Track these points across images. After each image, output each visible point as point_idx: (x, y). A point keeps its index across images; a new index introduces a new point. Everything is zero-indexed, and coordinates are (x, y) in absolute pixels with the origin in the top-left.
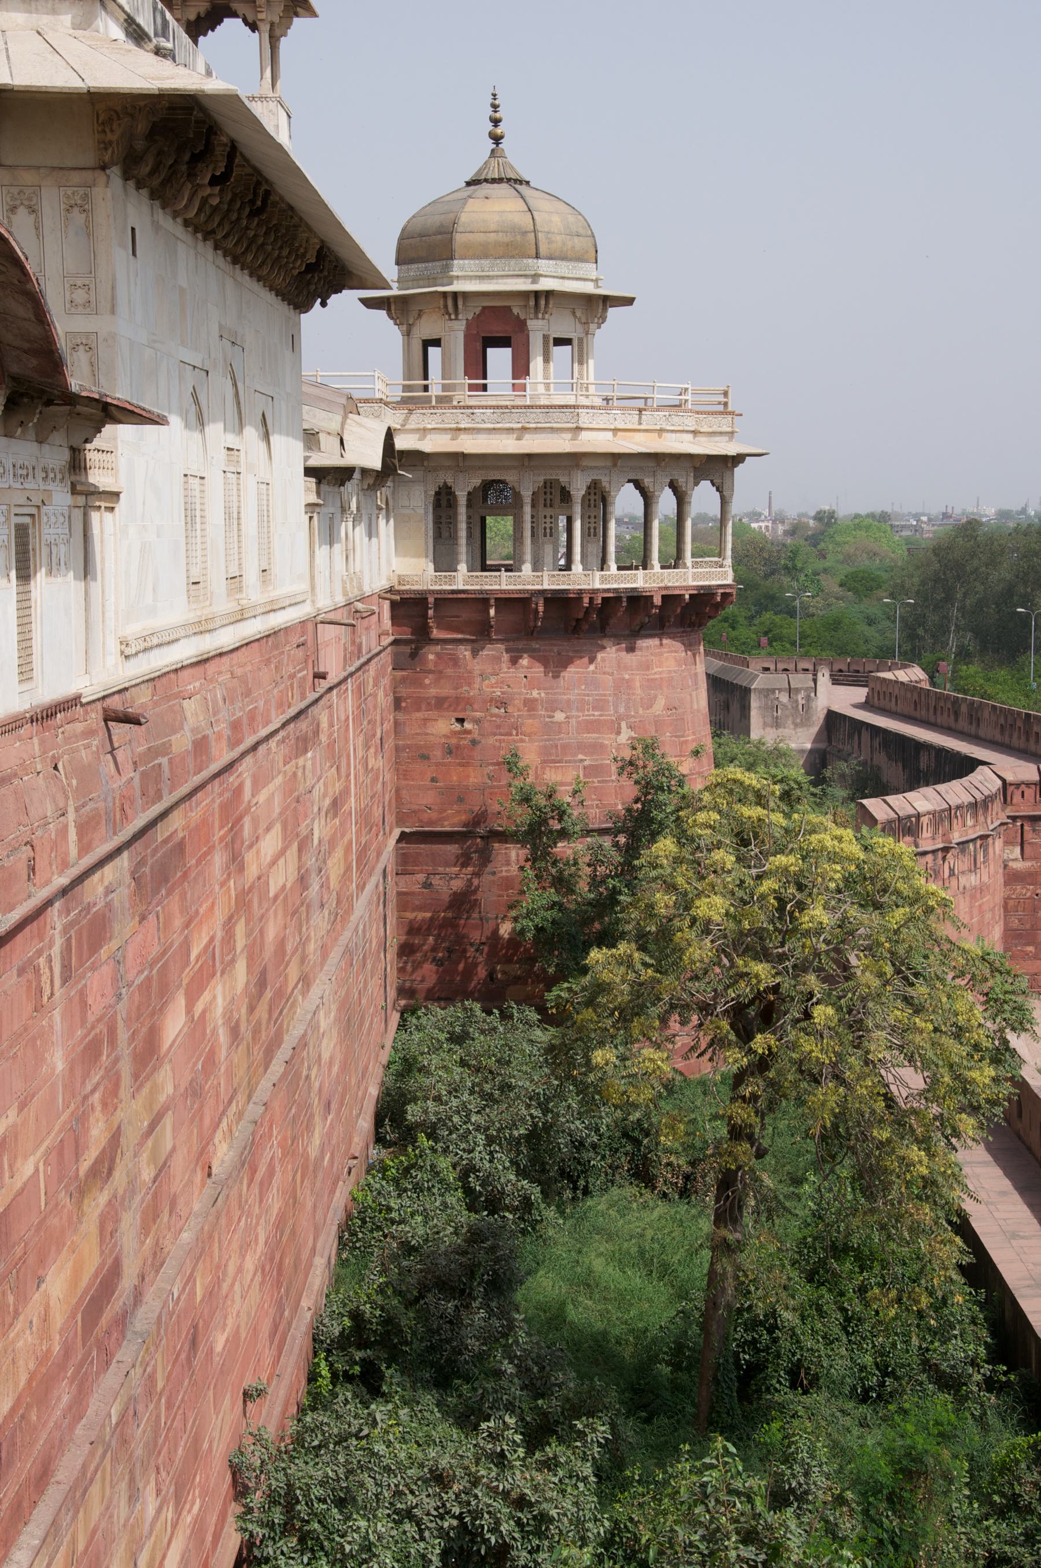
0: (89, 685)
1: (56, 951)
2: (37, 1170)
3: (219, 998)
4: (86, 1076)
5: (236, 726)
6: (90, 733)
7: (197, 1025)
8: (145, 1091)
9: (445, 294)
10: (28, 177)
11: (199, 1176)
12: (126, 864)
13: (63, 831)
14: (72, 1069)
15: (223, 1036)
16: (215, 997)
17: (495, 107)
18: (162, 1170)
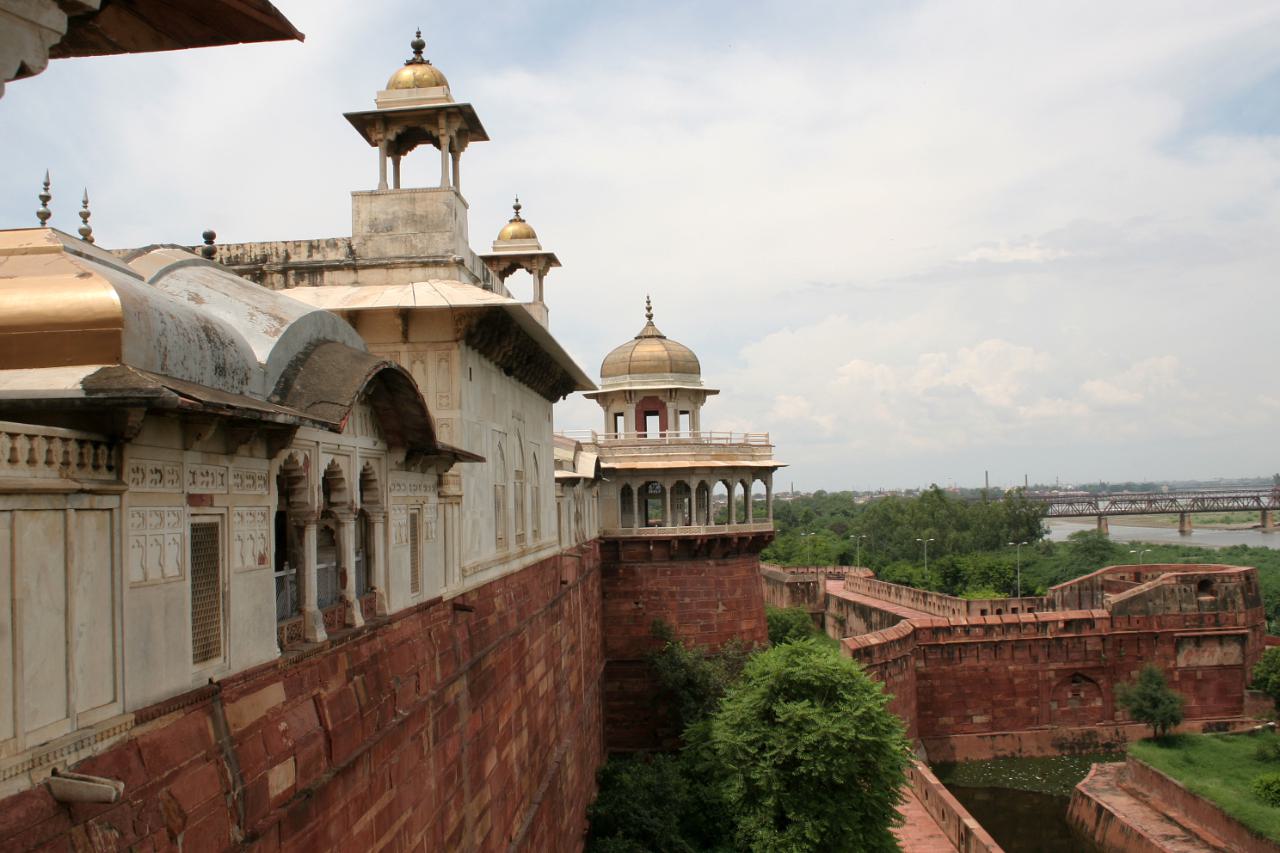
0: (449, 590)
1: (430, 728)
2: (423, 840)
3: (513, 749)
5: (521, 610)
7: (503, 764)
8: (477, 798)
9: (625, 391)
10: (421, 347)
11: (506, 841)
14: (439, 789)
15: (516, 770)
16: (512, 750)
17: (648, 302)
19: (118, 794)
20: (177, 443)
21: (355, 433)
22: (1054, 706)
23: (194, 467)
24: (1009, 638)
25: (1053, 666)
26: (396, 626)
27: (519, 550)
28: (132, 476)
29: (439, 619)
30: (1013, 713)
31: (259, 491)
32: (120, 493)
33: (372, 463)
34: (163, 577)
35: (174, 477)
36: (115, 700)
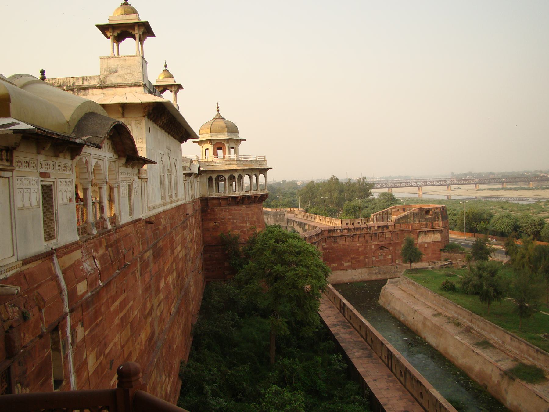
1: (139, 270)
3: (170, 279)
5: (171, 224)
7: (167, 284)
11: (169, 314)
15: (172, 287)
18: (162, 313)
19: (18, 291)
20: (35, 151)
22: (374, 258)
23: (42, 161)
24: (357, 233)
25: (373, 243)
26: (124, 229)
28: (17, 164)
29: (141, 227)
30: (359, 262)
31: (68, 172)
32: (12, 171)
34: (31, 206)
35: (34, 165)
36: (13, 255)
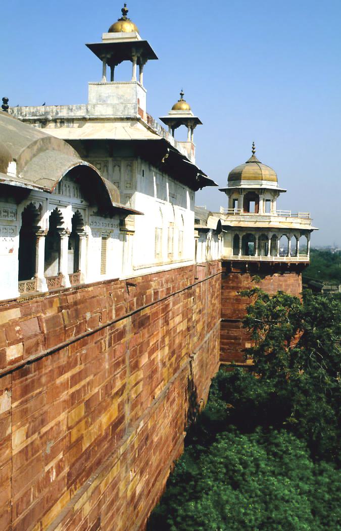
0: (123, 277)
1: (107, 338)
2: (99, 391)
3: (159, 356)
4: (115, 370)
5: (168, 289)
6: (122, 288)
7: (152, 362)
11: (150, 398)
12: (131, 320)
13: (111, 311)
14: (111, 368)
15: (160, 365)
16: (158, 355)
17: (254, 145)
18: (139, 396)
21: (70, 196)
26: (90, 289)
27: (169, 260)
29: (117, 288)
31: (10, 219)
33: (81, 212)
